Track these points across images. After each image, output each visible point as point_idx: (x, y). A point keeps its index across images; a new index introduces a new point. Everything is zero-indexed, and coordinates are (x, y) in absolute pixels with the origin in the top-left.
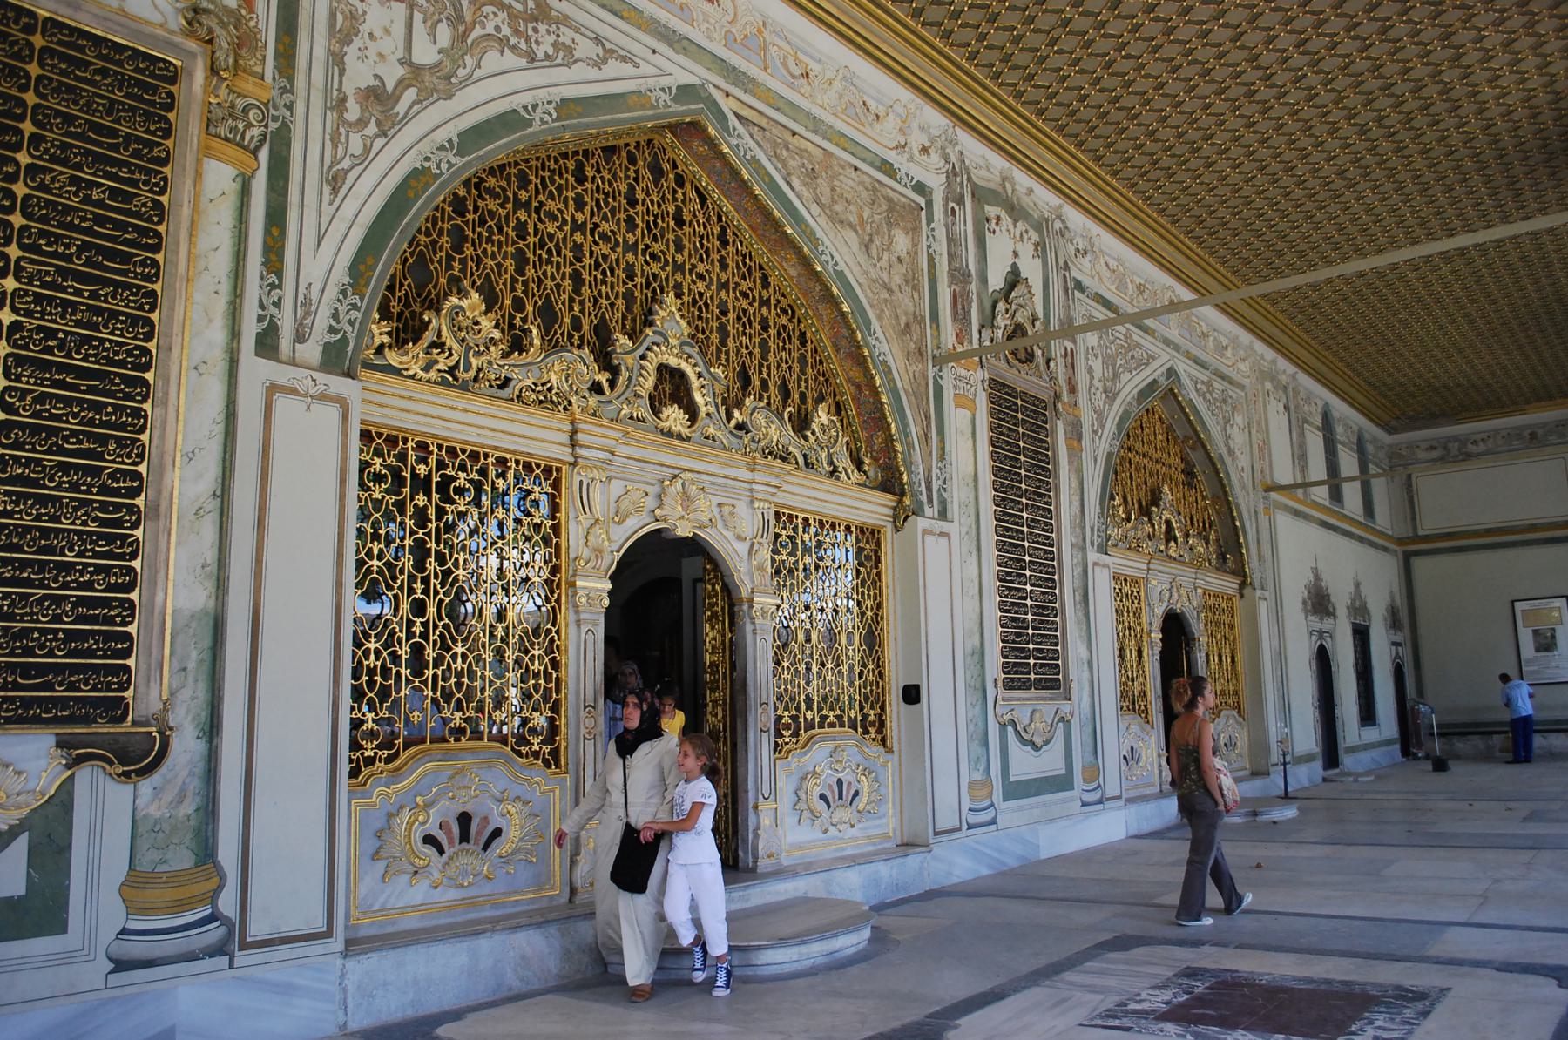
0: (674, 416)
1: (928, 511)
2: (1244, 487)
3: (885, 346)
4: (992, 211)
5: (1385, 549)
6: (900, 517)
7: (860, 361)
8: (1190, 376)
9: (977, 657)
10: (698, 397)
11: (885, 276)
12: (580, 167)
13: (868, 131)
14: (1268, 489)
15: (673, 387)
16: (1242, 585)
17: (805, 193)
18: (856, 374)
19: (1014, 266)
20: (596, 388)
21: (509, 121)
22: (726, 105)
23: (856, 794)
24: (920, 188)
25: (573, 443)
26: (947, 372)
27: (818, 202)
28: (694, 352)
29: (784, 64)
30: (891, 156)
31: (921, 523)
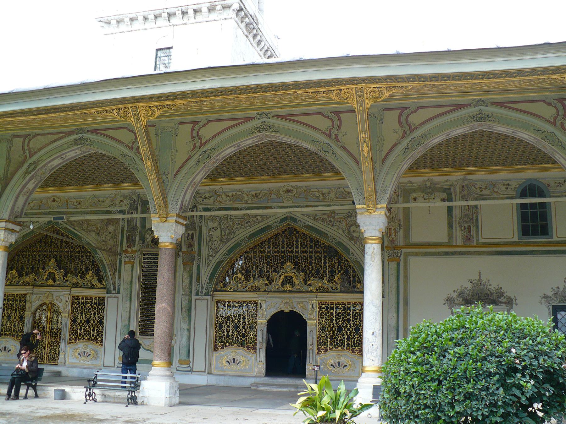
0: (50, 282)
1: (113, 292)
8: (308, 216)
9: (126, 327)
10: (57, 277)
11: (104, 239)
12: (41, 240)
13: (100, 206)
15: (52, 276)
17: (79, 229)
20: (35, 280)
23: (90, 355)
27: (83, 229)
28: (57, 268)
29: (73, 205)
30: (108, 209)
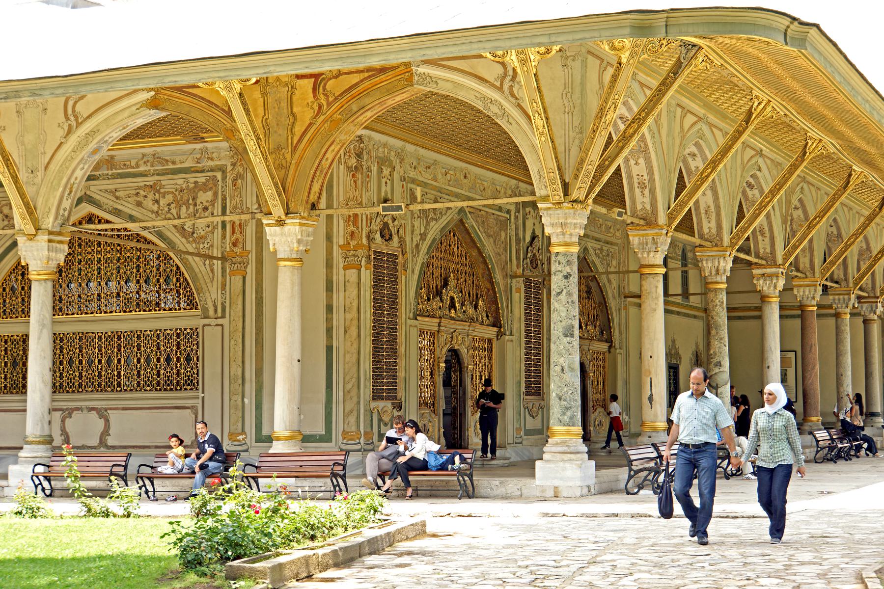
2: (614, 297)
3: (498, 277)
4: (527, 210)
5: (695, 317)
6: (499, 335)
7: (492, 283)
14: (625, 297)
16: (610, 347)
18: (489, 285)
19: (534, 230)
21: (434, 240)
22: (467, 210)
24: (508, 212)
25: (439, 326)
26: (514, 280)
31: (507, 338)
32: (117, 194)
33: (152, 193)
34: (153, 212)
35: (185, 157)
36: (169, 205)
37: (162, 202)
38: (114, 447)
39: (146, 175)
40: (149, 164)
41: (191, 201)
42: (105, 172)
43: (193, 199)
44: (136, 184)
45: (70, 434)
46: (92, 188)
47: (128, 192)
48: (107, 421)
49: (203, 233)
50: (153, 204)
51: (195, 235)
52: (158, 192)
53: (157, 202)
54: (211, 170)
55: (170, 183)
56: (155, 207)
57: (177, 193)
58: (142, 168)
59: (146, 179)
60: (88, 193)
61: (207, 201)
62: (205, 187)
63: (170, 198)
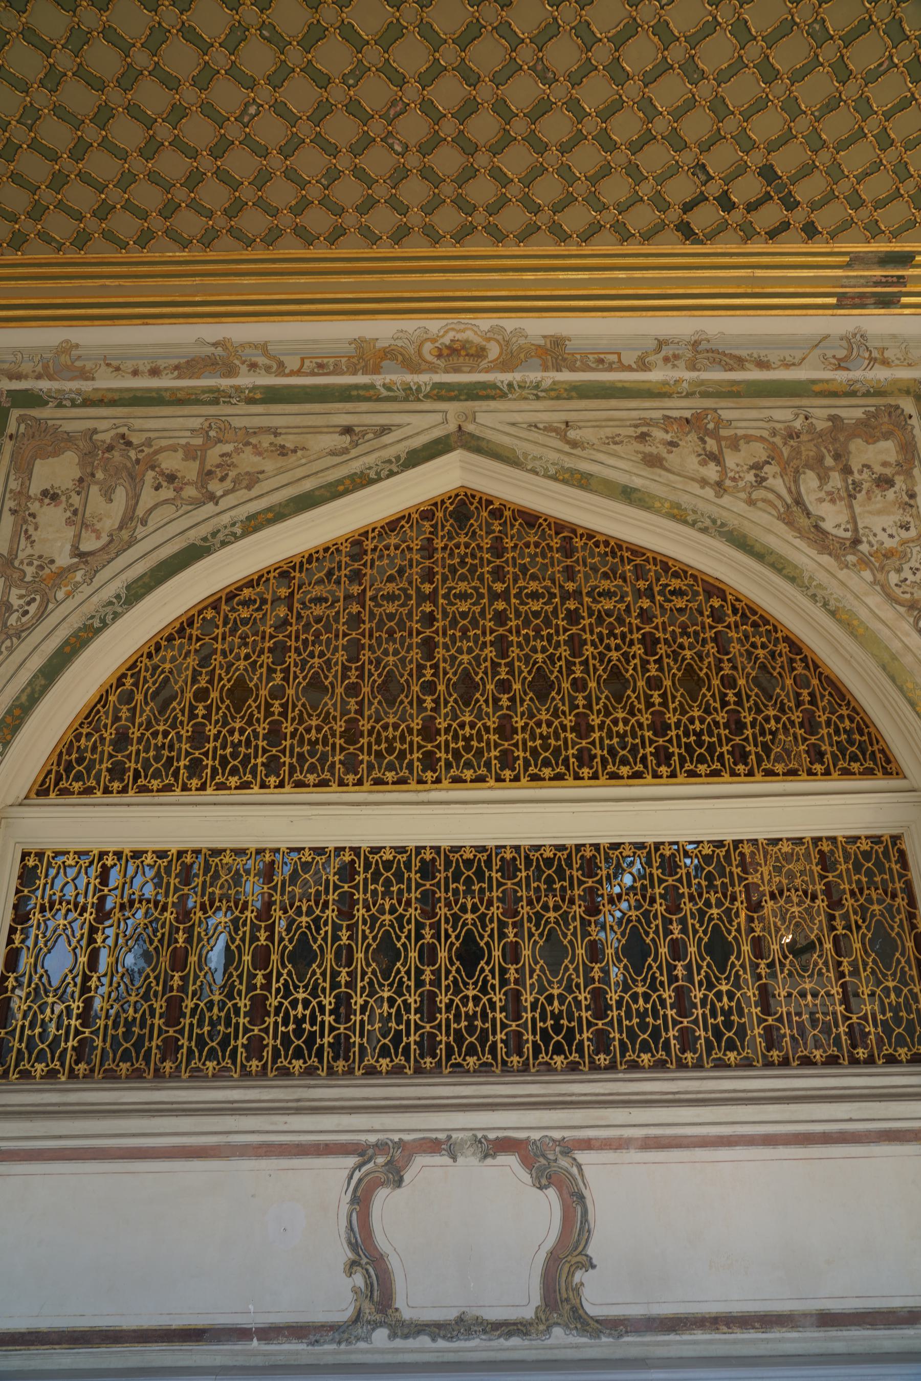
32: (572, 434)
33: (693, 437)
34: (704, 482)
35: (799, 355)
36: (757, 467)
37: (731, 460)
38: (617, 1326)
39: (668, 395)
40: (681, 363)
41: (829, 461)
42: (533, 376)
43: (837, 457)
44: (635, 414)
45: (394, 1263)
46: (481, 418)
47: (609, 432)
48: (575, 1202)
49: (889, 543)
50: (703, 463)
51: (864, 548)
52: (714, 434)
53: (716, 458)
54: (879, 393)
55: (742, 417)
56: (712, 472)
57: (778, 440)
58: (656, 376)
59: (668, 403)
60: (470, 428)
61: (885, 464)
62: (868, 429)
63: (759, 452)
